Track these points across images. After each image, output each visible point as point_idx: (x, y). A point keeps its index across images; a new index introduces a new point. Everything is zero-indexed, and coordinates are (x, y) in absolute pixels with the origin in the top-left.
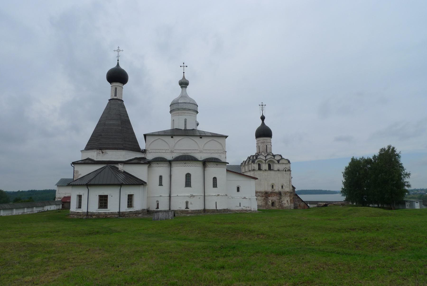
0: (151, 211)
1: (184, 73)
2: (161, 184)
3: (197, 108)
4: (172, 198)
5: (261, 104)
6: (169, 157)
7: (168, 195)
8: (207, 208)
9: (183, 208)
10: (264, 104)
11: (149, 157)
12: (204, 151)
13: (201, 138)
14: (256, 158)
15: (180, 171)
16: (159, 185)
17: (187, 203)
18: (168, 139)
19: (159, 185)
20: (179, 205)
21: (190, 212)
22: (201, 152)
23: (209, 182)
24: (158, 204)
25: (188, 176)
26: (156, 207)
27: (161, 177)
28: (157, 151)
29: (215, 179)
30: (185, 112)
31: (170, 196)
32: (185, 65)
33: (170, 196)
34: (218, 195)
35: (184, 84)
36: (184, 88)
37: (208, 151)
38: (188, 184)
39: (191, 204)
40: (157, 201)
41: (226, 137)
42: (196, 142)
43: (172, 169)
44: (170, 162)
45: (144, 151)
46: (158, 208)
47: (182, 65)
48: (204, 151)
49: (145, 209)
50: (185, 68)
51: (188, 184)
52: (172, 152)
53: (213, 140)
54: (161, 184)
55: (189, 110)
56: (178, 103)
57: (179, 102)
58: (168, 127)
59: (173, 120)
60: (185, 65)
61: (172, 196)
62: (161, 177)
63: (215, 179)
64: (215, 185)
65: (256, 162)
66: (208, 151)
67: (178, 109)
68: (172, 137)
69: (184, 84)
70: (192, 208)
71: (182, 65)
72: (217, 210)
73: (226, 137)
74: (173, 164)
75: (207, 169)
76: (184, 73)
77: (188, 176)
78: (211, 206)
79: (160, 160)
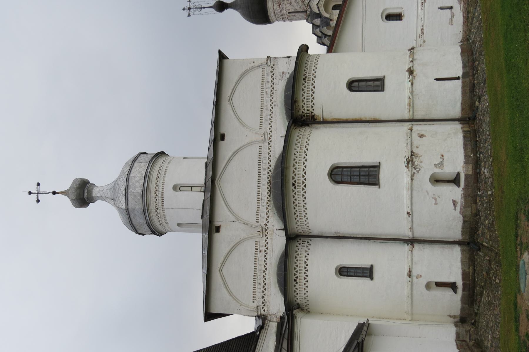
0: (462, 309)
1: (54, 193)
2: (367, 273)
3: (150, 154)
4: (419, 233)
5: (186, 12)
6: (278, 242)
7: (407, 248)
8: (456, 111)
9: (456, 193)
10: (187, 5)
11: (277, 306)
12: (266, 126)
13: (223, 137)
14: (319, 16)
15: (323, 203)
16: (371, 278)
17: (436, 180)
18: (222, 241)
19: (371, 278)
20: (445, 210)
21: (470, 167)
22: (267, 138)
23: (365, 103)
24: (439, 284)
25: (340, 175)
26: (448, 293)
27: (343, 271)
28: (260, 280)
29: (354, 85)
30: (152, 190)
31: (412, 242)
32: (34, 189)
33: (412, 242)
34: (411, 72)
35: (83, 194)
36: (95, 193)
37: (266, 113)
38: (366, 175)
39: (440, 165)
40: (428, 286)
41: (222, 57)
42: (235, 153)
43: (315, 232)
44: (292, 238)
45: (263, 320)
46: (453, 286)
47: (34, 197)
48: (266, 126)
49: (458, 335)
50: (42, 189)
51: (366, 175)
52: (264, 231)
53: (230, 99)
54: (367, 273)
55: (147, 176)
56: (127, 209)
57: (124, 207)
58: (196, 240)
59: (179, 225)
60: (34, 189)
61: (408, 234)
62: (343, 271)
63: (354, 85)
64: (376, 85)
65: (327, 16)
66: (266, 113)
67: (145, 210)
68: (218, 229)
69: (83, 194)
70: (456, 162)
71: (34, 197)
72: (465, 75)
73: (222, 57)
74: (298, 227)
75: (317, 112)
76: (54, 193)
77: (340, 175)
78: (451, 98)
79: (286, 274)
